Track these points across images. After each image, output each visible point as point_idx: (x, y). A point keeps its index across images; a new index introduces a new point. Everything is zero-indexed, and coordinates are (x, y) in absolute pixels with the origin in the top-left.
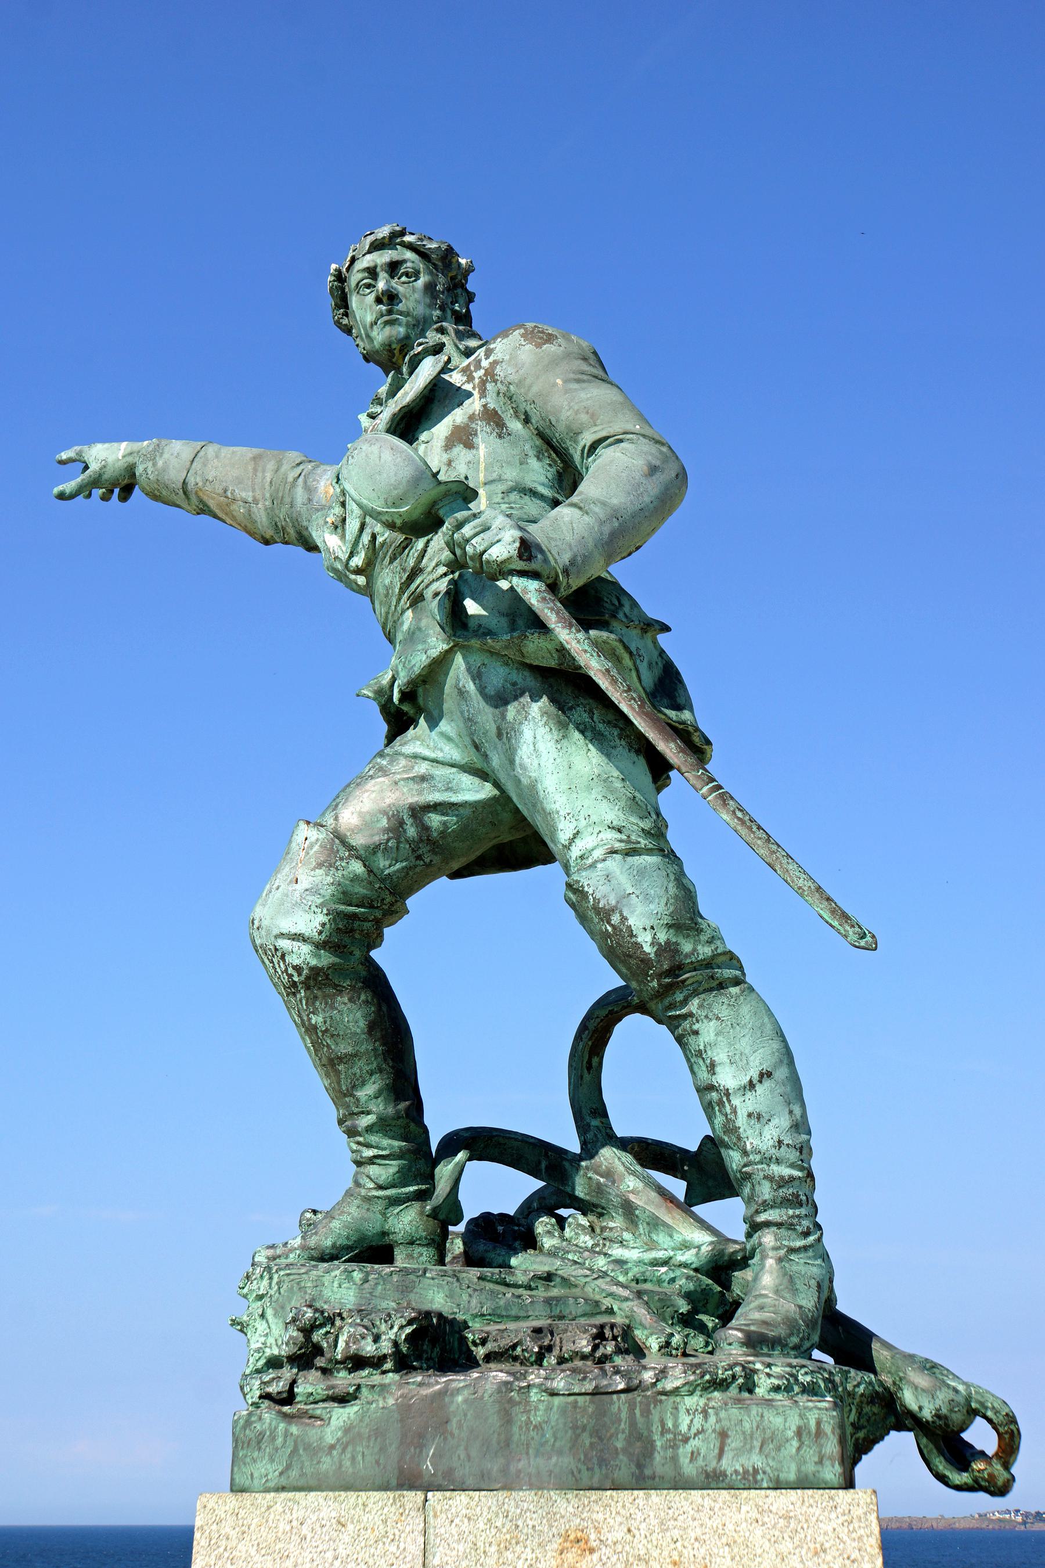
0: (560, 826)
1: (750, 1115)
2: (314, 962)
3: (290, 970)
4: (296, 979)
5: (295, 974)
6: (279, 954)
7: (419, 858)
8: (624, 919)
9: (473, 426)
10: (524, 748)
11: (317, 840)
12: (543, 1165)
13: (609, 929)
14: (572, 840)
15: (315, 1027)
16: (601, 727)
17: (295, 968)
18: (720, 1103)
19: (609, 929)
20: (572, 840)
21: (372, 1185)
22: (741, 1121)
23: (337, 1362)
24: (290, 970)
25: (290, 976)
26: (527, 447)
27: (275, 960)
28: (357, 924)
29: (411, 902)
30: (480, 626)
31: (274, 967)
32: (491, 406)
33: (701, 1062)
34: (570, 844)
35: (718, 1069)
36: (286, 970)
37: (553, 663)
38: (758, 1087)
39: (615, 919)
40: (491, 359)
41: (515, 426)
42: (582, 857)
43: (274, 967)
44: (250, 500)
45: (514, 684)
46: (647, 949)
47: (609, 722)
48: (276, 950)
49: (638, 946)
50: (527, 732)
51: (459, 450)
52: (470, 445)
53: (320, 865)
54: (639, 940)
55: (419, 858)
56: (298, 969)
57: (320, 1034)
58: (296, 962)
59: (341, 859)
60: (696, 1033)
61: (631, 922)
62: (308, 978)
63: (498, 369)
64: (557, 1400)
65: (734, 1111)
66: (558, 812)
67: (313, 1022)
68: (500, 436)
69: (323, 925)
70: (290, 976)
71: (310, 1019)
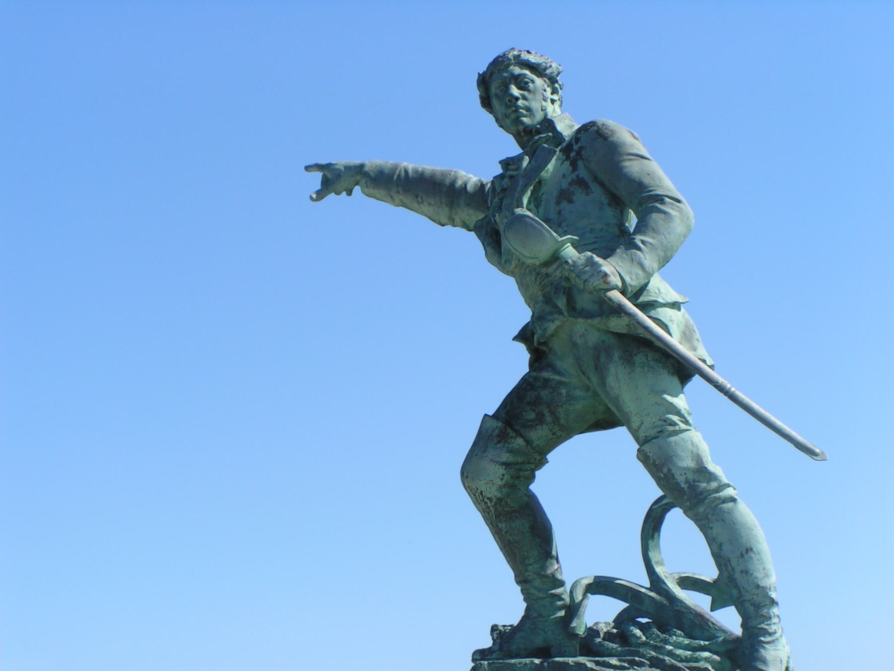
0: (633, 420)
1: (742, 572)
2: (499, 495)
7: (554, 434)
8: (669, 470)
9: (572, 189)
12: (629, 596)
14: (639, 427)
15: (501, 530)
16: (652, 363)
17: (488, 498)
18: (726, 565)
20: (639, 427)
22: (737, 575)
25: (486, 503)
26: (603, 198)
28: (521, 474)
29: (549, 457)
30: (583, 309)
32: (581, 176)
35: (724, 547)
37: (624, 332)
38: (746, 556)
39: (665, 470)
40: (579, 144)
41: (595, 188)
45: (603, 342)
46: (683, 485)
47: (657, 360)
49: (678, 484)
50: (612, 369)
51: (565, 204)
52: (570, 201)
53: (499, 442)
54: (679, 480)
55: (554, 434)
56: (490, 499)
58: (489, 496)
59: (511, 438)
60: (711, 528)
61: (673, 471)
62: (496, 504)
63: (583, 152)
65: (733, 570)
68: (587, 194)
69: (503, 475)
70: (486, 503)
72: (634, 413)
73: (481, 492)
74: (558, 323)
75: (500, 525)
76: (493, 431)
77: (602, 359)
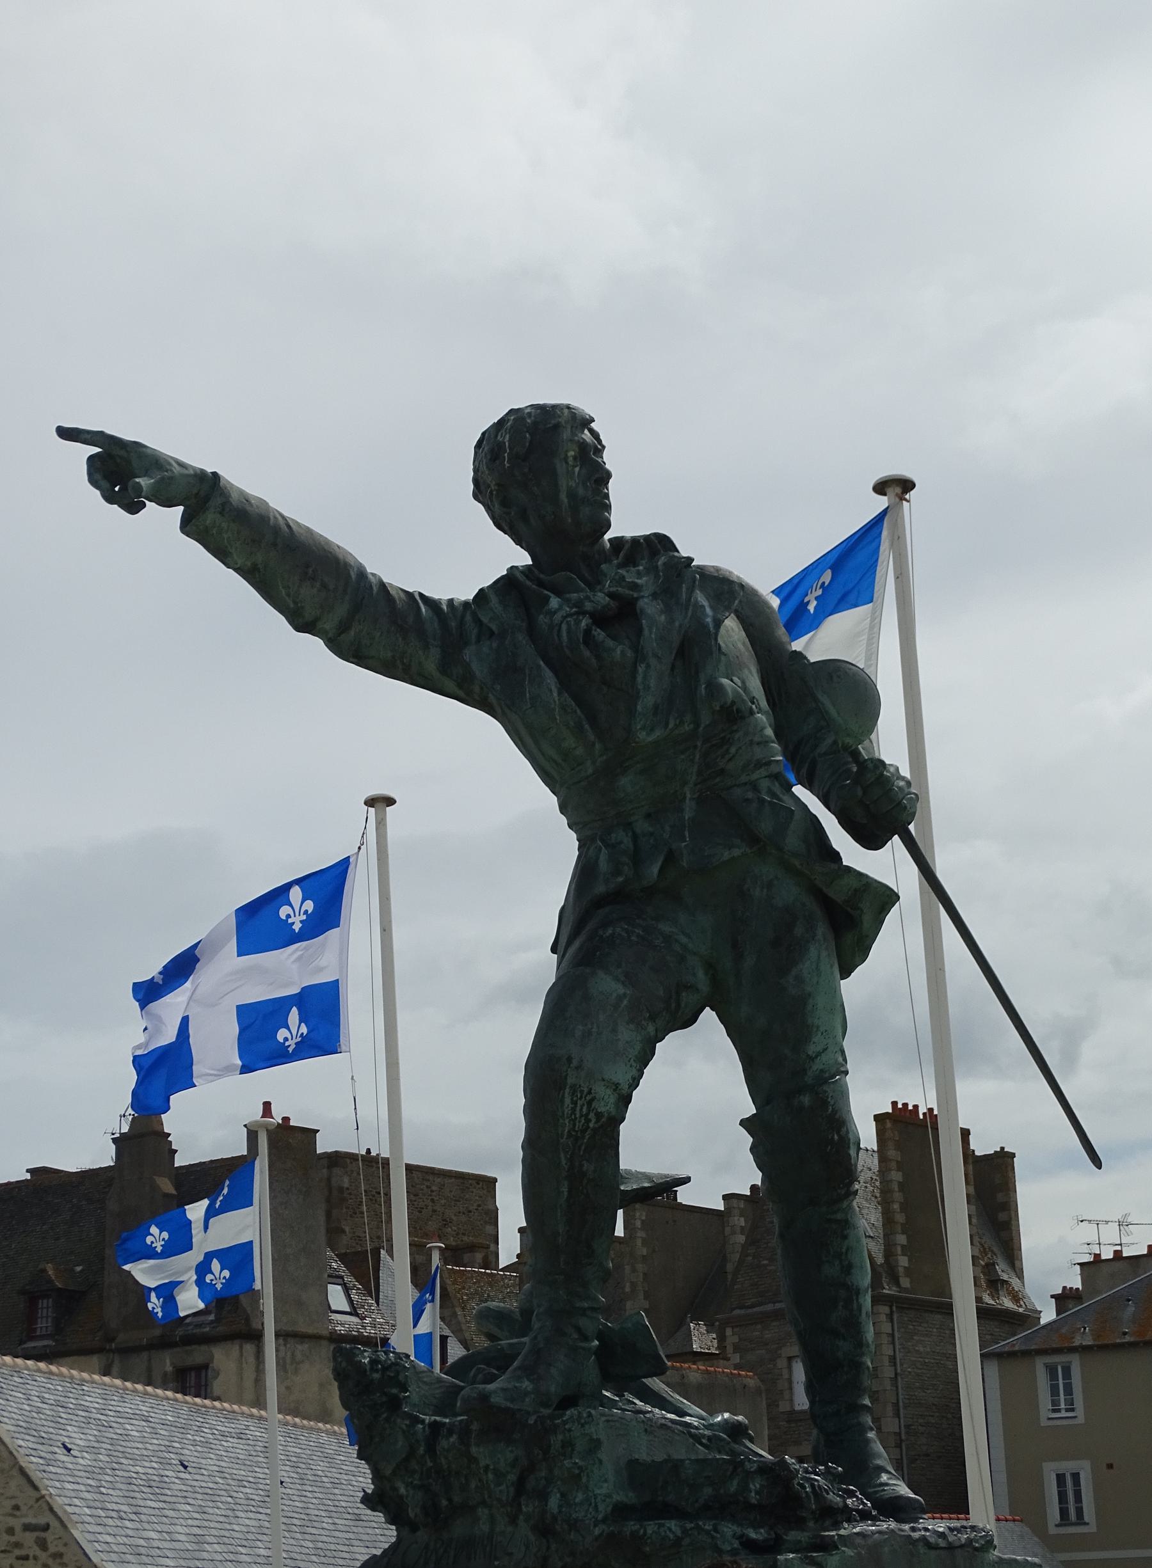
3: (592, 1116)
4: (591, 1125)
5: (594, 1120)
6: (588, 1098)
10: (808, 964)
11: (625, 995)
13: (836, 1137)
14: (819, 1054)
19: (836, 1137)
20: (819, 1054)
21: (576, 1336)
23: (813, 1512)
24: (592, 1116)
27: (579, 1103)
31: (574, 1110)
33: (837, 1263)
34: (816, 1057)
36: (587, 1114)
42: (822, 1071)
43: (574, 1110)
44: (331, 587)
48: (590, 1092)
50: (813, 952)
56: (599, 1116)
57: (585, 1181)
64: (933, 1553)
66: (818, 1027)
67: (585, 1168)
71: (581, 1166)
72: (822, 1029)
73: (590, 1103)
74: (736, 852)
75: (586, 1165)
76: (620, 998)
77: (799, 931)
